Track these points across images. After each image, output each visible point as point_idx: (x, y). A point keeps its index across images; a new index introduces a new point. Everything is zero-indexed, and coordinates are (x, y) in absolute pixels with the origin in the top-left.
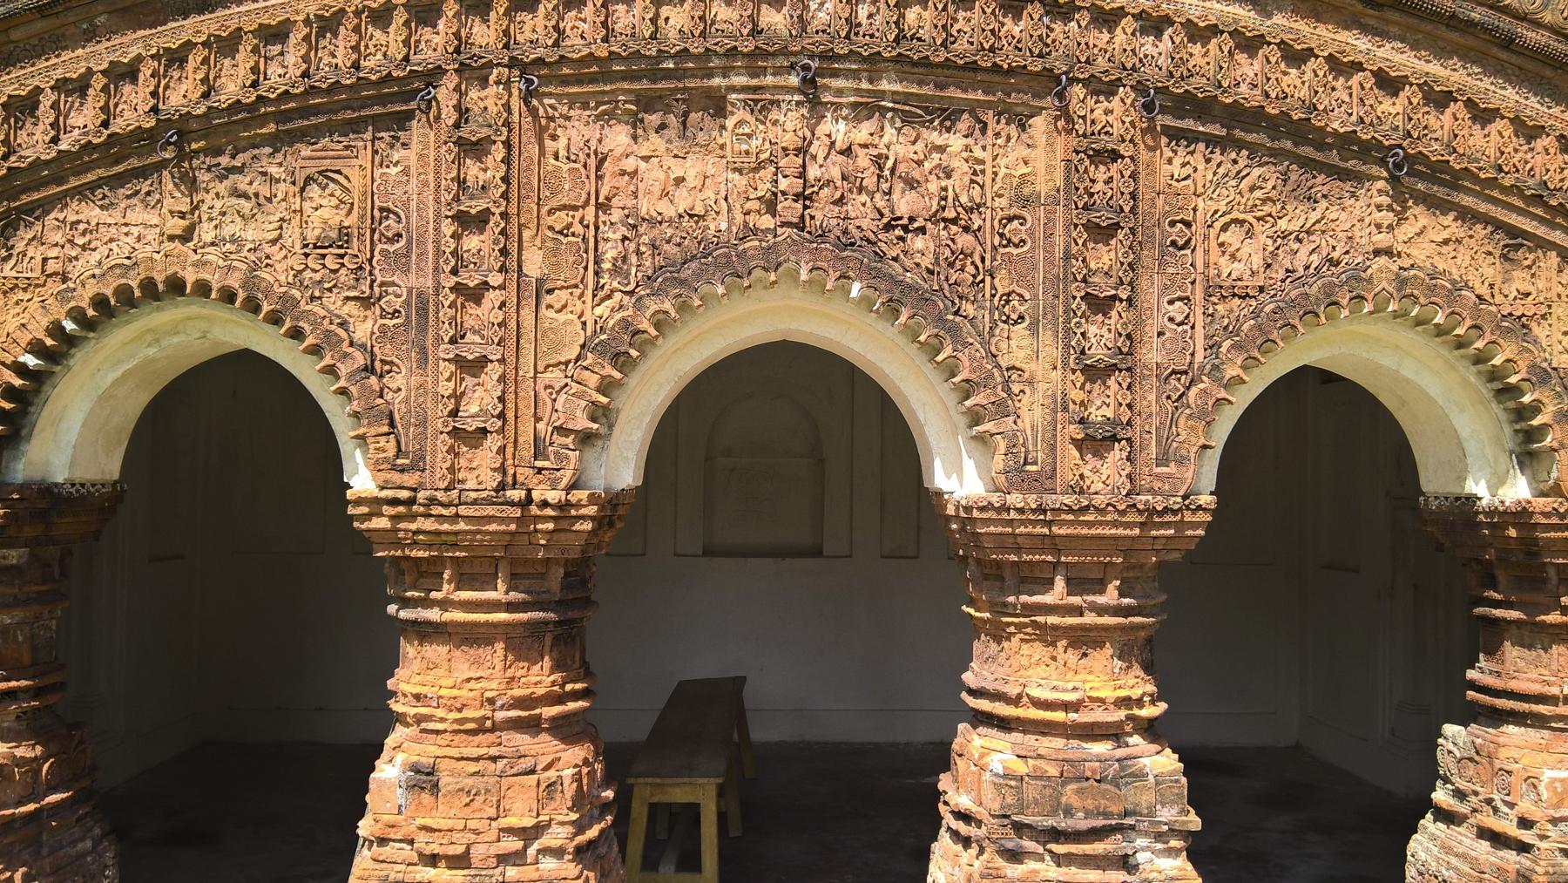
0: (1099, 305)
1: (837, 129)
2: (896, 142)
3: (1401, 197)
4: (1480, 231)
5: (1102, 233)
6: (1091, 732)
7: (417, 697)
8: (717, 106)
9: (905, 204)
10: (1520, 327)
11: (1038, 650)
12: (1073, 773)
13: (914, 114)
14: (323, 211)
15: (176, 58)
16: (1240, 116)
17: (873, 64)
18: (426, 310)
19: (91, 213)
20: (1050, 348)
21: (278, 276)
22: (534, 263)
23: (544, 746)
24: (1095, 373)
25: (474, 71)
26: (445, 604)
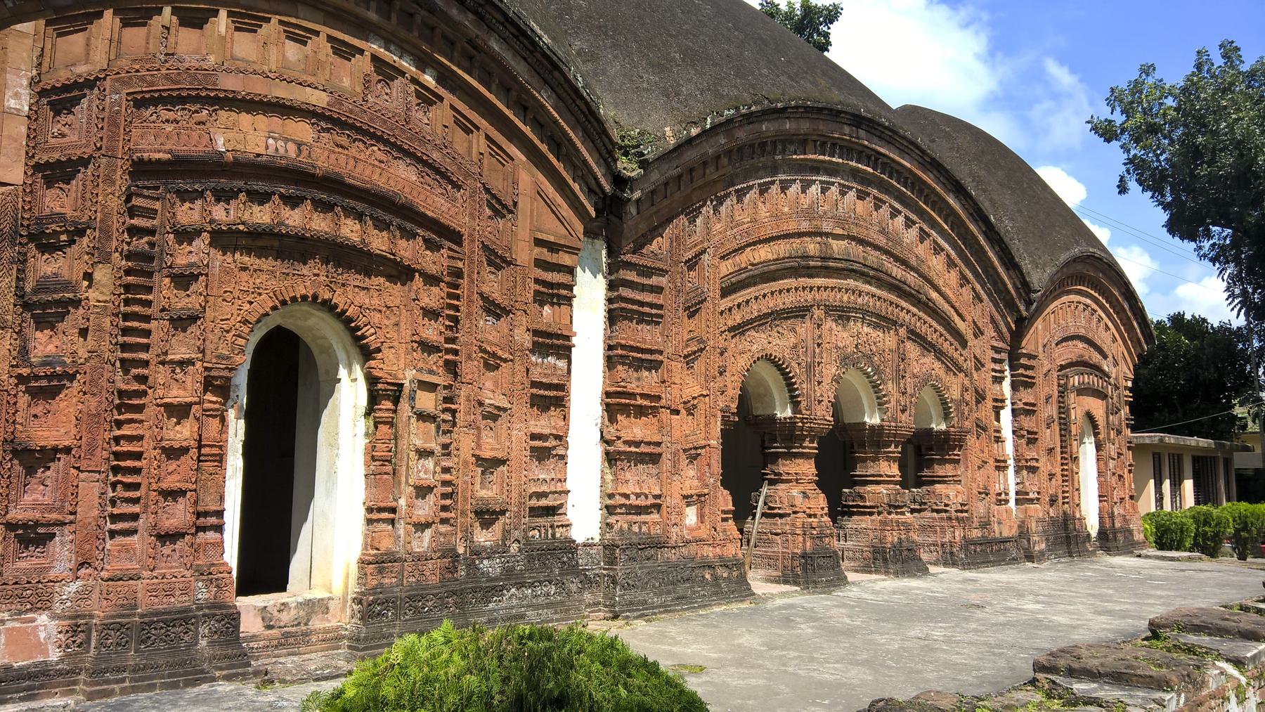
4: (944, 366)
7: (796, 474)
8: (848, 319)
11: (886, 463)
18: (810, 367)
19: (753, 333)
26: (805, 448)
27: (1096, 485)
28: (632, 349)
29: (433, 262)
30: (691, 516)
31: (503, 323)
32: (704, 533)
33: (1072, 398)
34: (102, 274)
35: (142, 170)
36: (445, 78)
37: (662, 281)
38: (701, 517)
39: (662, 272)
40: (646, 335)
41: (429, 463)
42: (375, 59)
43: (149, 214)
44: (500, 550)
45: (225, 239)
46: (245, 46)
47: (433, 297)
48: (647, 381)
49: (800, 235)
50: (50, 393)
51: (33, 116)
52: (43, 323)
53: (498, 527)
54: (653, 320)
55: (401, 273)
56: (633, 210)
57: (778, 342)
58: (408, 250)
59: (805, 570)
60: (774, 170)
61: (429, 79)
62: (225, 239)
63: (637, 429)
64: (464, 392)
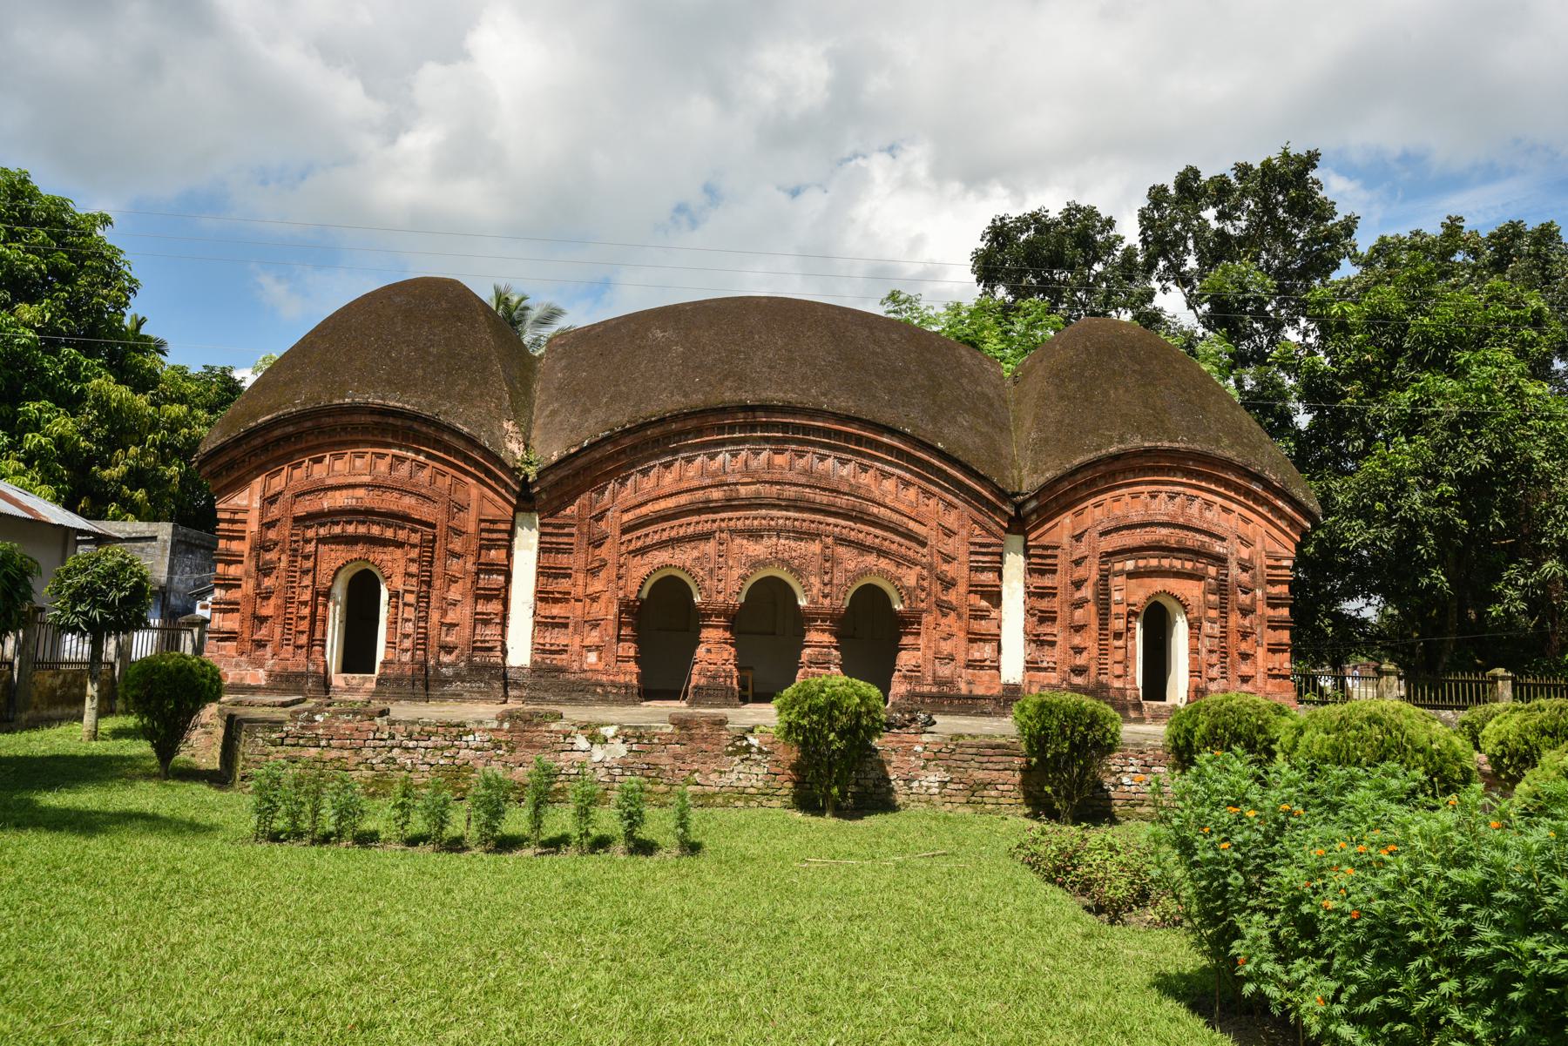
0: (826, 573)
1: (782, 541)
2: (792, 543)
3: (878, 556)
5: (827, 561)
6: (824, 647)
8: (762, 537)
9: (794, 554)
10: (899, 579)
12: (820, 653)
13: (795, 539)
14: (696, 553)
15: (672, 528)
16: (850, 541)
17: (789, 531)
20: (818, 580)
21: (688, 564)
22: (730, 563)
23: (728, 647)
24: (825, 585)
25: (722, 531)
27: (1187, 661)
28: (550, 568)
29: (415, 538)
30: (592, 658)
31: (461, 561)
32: (601, 666)
33: (1118, 581)
34: (284, 557)
35: (297, 520)
36: (429, 456)
37: (574, 530)
38: (600, 659)
39: (573, 526)
40: (563, 560)
41: (411, 624)
42: (394, 456)
43: (297, 535)
44: (453, 664)
45: (322, 541)
46: (339, 465)
47: (414, 554)
48: (564, 584)
49: (704, 488)
50: (268, 598)
51: (262, 507)
52: (266, 575)
53: (454, 654)
54: (569, 551)
55: (400, 545)
56: (544, 496)
57: (683, 557)
58: (402, 535)
59: (695, 694)
60: (675, 451)
61: (421, 458)
62: (322, 541)
63: (556, 610)
64: (434, 595)
